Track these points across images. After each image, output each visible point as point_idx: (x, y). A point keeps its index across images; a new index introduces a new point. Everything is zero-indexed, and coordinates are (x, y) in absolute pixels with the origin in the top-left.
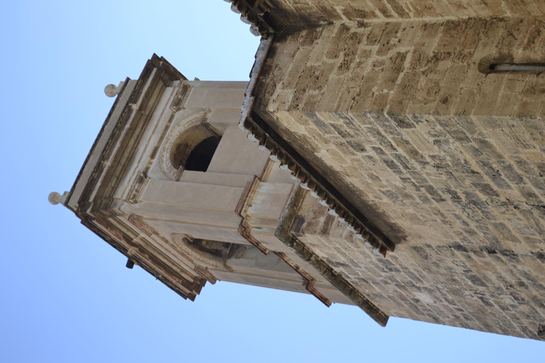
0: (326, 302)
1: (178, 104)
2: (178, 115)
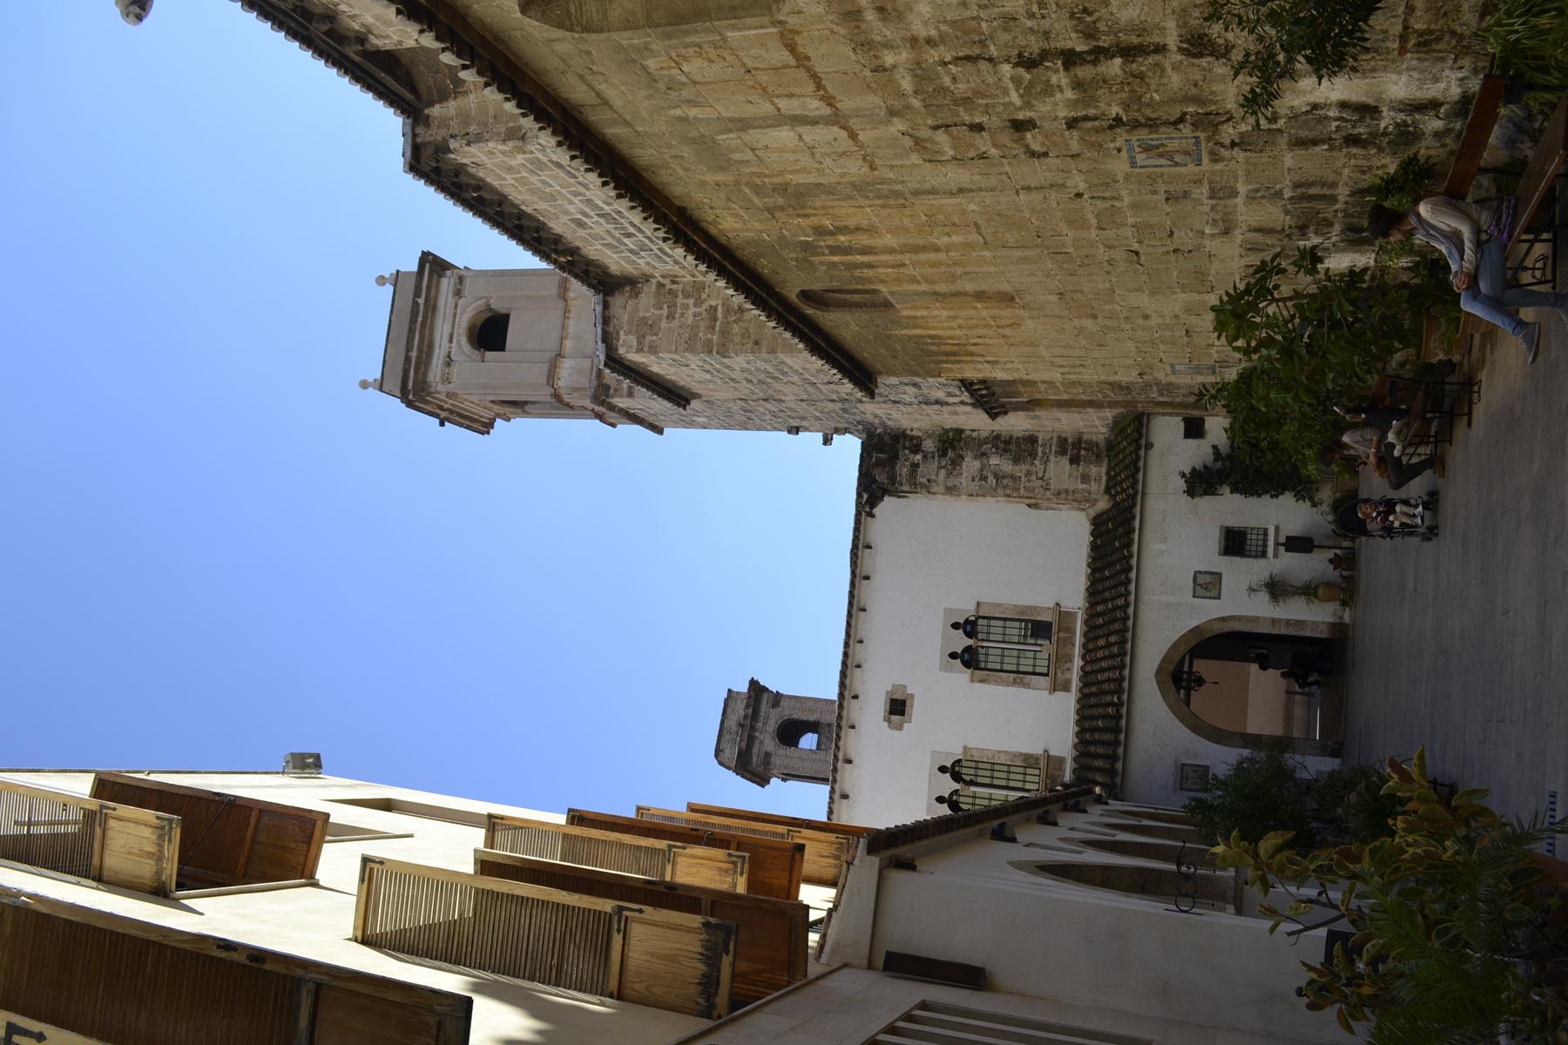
0: (613, 425)
1: (458, 293)
2: (461, 302)
